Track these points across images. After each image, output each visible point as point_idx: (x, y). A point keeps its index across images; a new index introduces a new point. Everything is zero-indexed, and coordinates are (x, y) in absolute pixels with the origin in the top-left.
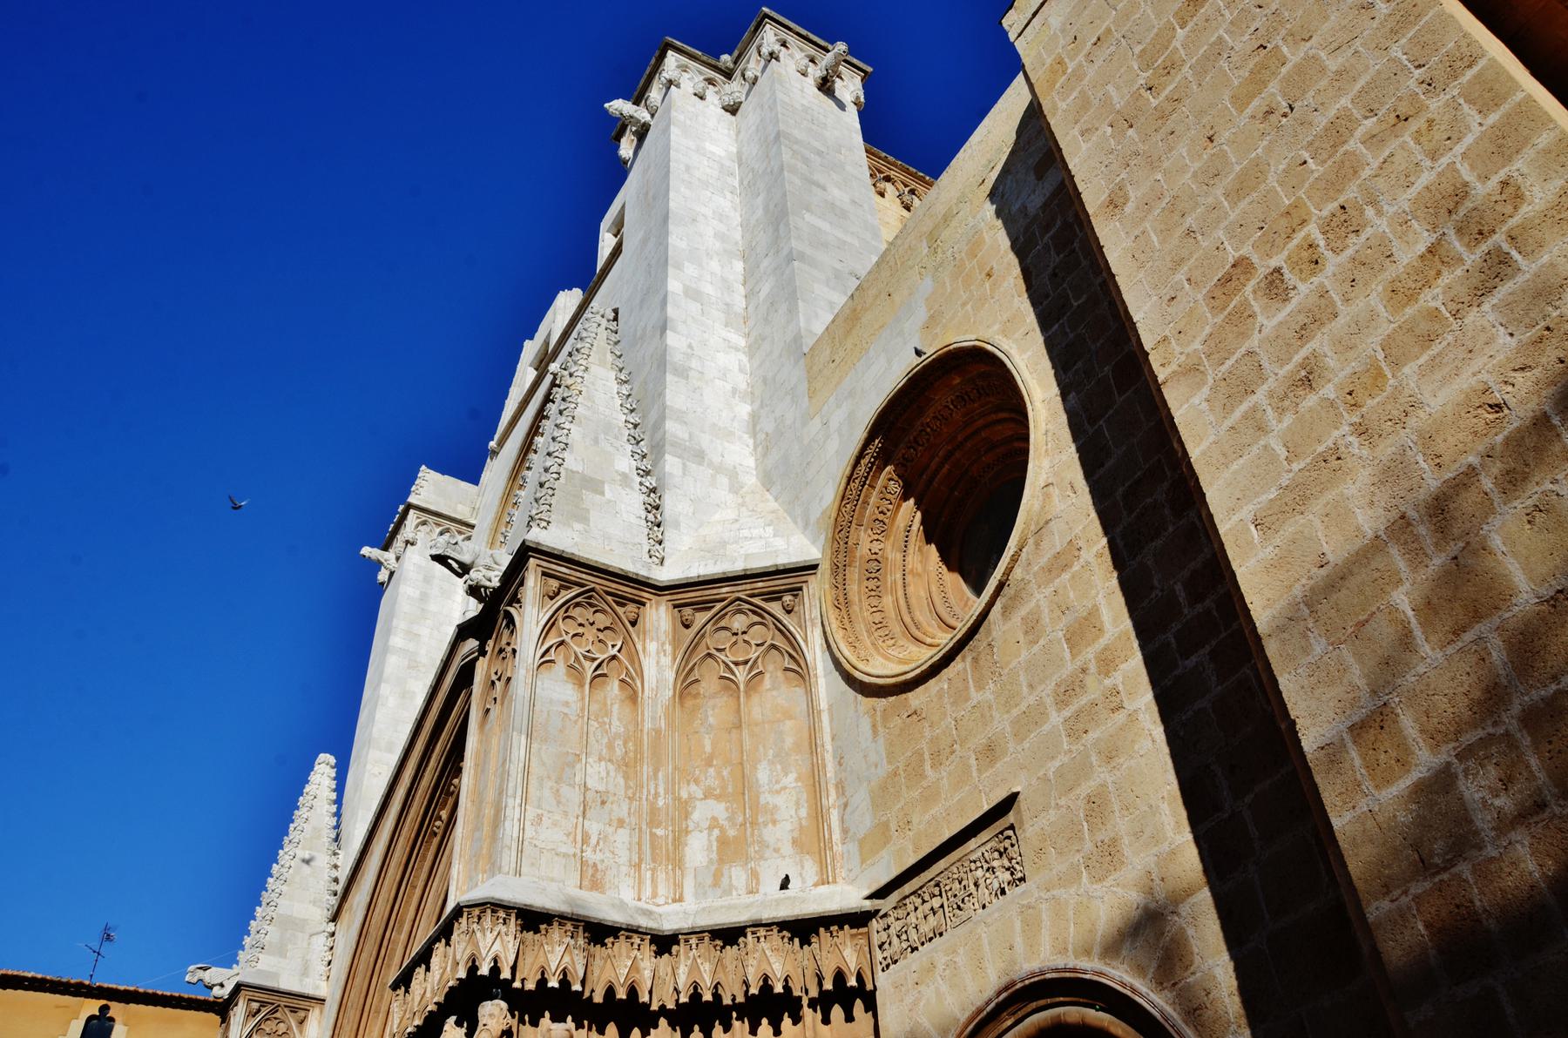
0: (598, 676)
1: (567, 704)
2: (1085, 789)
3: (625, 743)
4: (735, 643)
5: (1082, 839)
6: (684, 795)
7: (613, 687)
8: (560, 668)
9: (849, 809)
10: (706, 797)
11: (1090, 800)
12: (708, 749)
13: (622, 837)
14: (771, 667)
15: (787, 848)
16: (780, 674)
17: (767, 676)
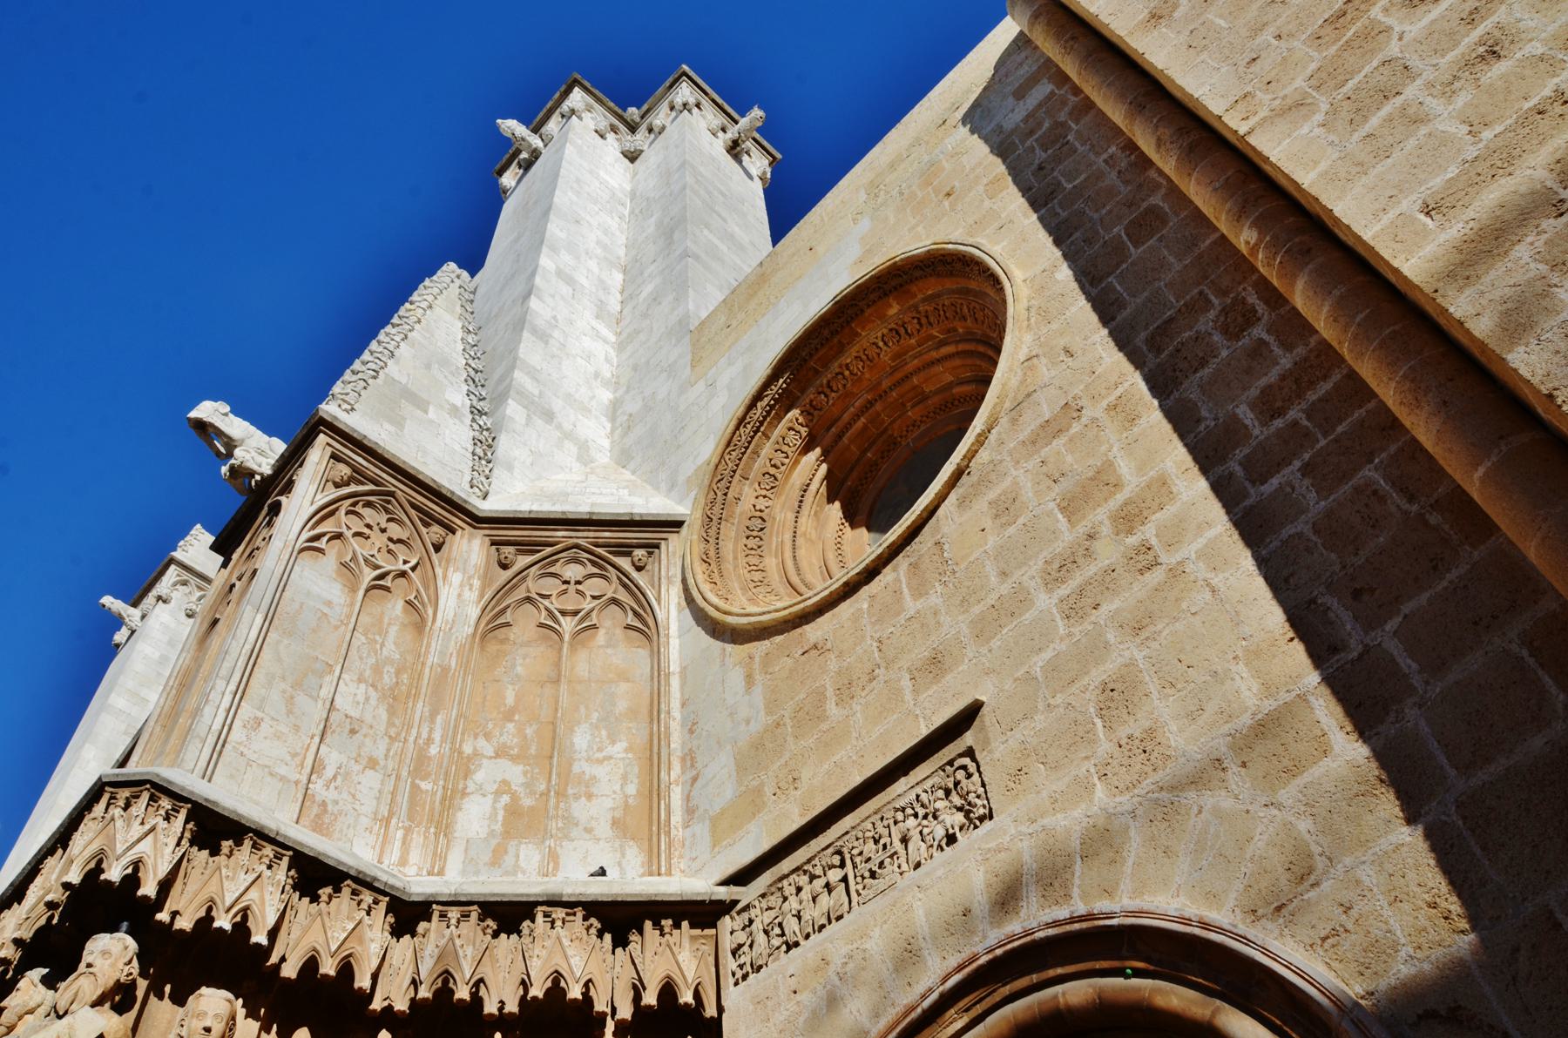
0: (379, 585)
1: (329, 604)
2: (1097, 675)
3: (398, 673)
4: (565, 592)
5: (1094, 742)
6: (468, 749)
7: (394, 607)
8: (330, 561)
9: (698, 784)
10: (497, 755)
11: (1107, 689)
12: (510, 699)
13: (370, 782)
14: (608, 623)
15: (604, 829)
16: (619, 632)
17: (602, 632)
